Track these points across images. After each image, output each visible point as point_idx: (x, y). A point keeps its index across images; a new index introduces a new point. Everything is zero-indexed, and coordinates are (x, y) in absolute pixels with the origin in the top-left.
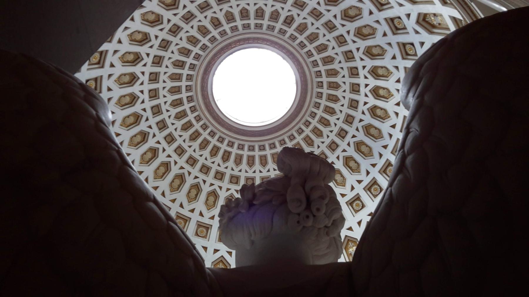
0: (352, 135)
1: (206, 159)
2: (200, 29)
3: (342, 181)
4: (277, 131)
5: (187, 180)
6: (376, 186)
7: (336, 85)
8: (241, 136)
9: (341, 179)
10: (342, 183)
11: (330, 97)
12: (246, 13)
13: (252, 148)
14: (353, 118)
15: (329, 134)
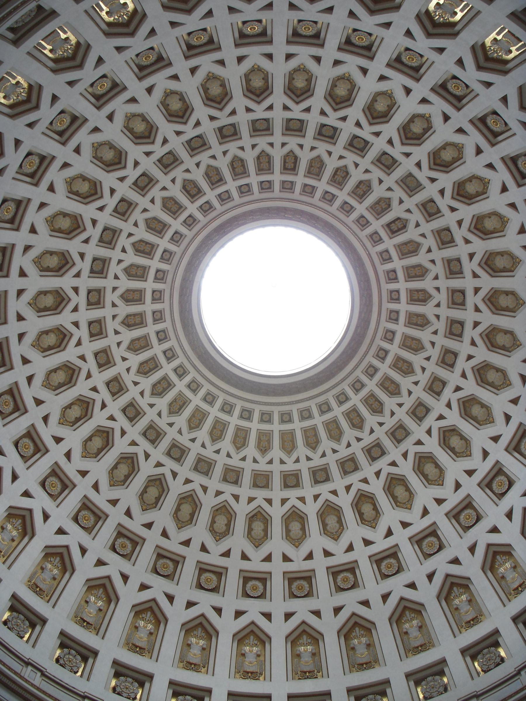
0: (390, 461)
1: (128, 370)
2: (261, 158)
3: (335, 530)
4: (267, 394)
5: (78, 383)
6: (392, 561)
7: (407, 368)
8: (207, 370)
9: (335, 526)
10: (335, 533)
11: (386, 382)
12: (342, 177)
13: (211, 399)
14: (408, 433)
15: (353, 442)
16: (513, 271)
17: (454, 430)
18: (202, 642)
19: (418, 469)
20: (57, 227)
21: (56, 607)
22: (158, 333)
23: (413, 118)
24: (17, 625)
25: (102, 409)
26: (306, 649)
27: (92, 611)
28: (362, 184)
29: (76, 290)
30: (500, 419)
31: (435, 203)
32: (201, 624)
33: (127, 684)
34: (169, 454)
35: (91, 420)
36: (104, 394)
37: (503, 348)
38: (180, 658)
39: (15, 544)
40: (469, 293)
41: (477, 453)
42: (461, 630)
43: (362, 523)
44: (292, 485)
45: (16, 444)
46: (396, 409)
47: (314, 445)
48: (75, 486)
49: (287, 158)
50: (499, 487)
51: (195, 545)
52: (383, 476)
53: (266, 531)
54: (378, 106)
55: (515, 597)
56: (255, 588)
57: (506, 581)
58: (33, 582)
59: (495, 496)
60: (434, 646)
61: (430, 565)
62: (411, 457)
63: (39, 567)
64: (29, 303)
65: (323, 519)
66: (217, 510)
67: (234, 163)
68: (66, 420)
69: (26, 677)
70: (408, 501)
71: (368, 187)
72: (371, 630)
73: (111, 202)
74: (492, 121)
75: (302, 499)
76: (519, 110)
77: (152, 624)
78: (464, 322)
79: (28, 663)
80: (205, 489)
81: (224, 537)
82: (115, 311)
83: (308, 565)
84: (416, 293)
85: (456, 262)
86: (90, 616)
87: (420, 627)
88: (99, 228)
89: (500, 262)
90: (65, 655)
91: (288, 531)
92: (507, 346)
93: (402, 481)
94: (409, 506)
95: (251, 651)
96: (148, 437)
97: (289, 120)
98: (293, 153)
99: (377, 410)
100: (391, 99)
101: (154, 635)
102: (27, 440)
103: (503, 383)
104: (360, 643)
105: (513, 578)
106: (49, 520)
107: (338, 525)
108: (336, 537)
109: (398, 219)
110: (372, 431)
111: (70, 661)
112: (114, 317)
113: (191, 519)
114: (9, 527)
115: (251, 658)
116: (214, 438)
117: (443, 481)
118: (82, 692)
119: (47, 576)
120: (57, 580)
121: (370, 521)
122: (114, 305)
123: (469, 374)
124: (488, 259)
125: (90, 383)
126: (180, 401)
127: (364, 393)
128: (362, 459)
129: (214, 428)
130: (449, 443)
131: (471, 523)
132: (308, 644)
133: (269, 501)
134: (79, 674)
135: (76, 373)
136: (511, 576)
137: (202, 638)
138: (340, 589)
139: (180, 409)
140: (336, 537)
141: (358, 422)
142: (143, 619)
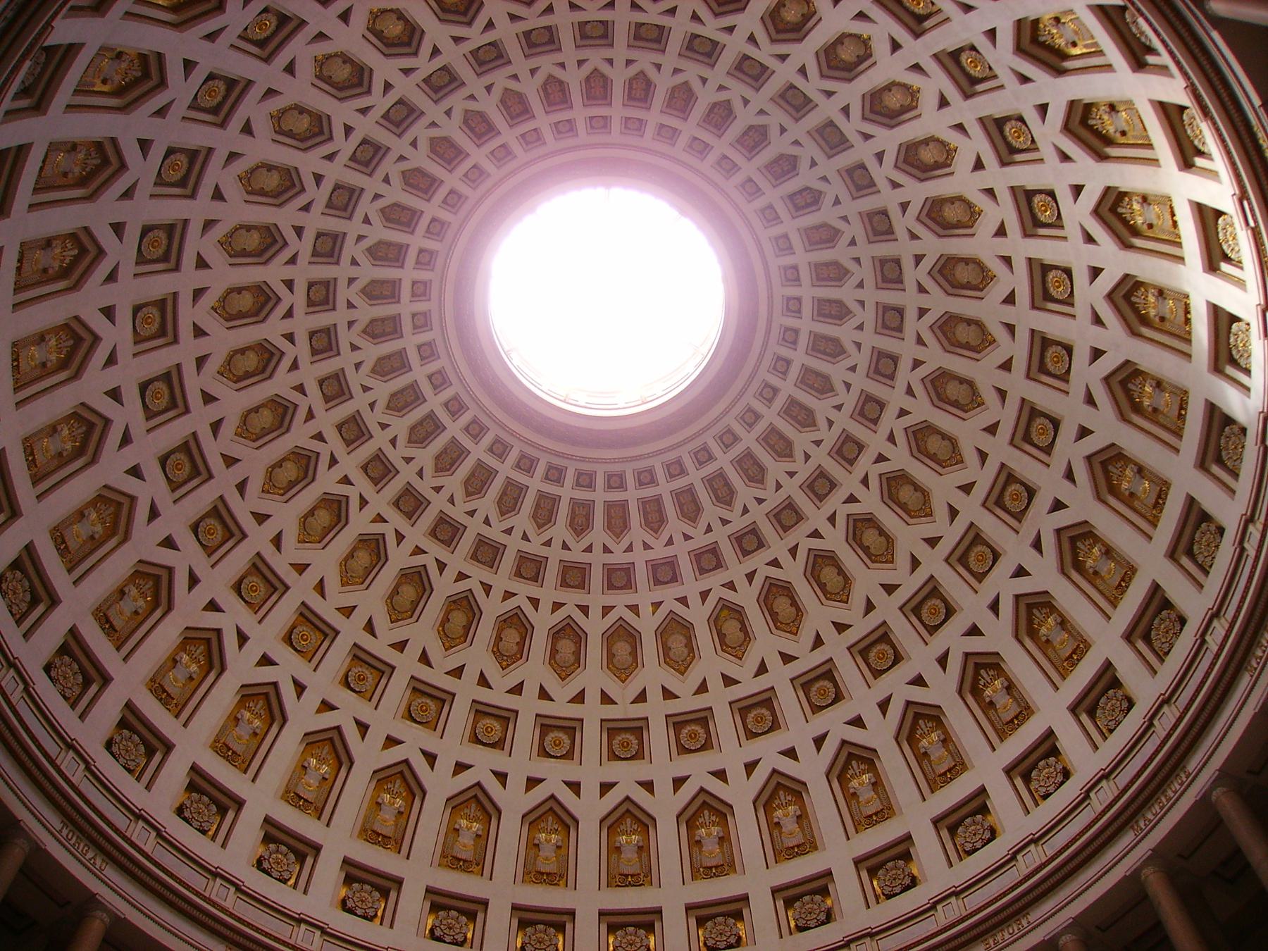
1: (372, 405)
2: (592, 80)
3: (682, 658)
14: (800, 517)
15: (716, 525)
16: (982, 290)
17: (869, 520)
18: (476, 826)
20: (257, 187)
21: (258, 781)
22: (419, 347)
23: (841, 39)
24: (199, 813)
25: (330, 467)
26: (629, 840)
27: (312, 781)
28: (754, 130)
29: (289, 284)
30: (941, 512)
31: (867, 170)
32: (475, 796)
33: (363, 894)
34: (433, 533)
35: (313, 484)
36: (335, 443)
37: (955, 404)
38: (443, 851)
39: (195, 683)
40: (911, 314)
41: (903, 561)
42: (858, 827)
43: (723, 650)
44: (620, 585)
45: (195, 528)
46: (784, 480)
48: (287, 588)
49: (634, 82)
50: (931, 616)
51: (470, 675)
52: (758, 580)
53: (577, 654)
54: (786, 14)
55: (941, 787)
56: (557, 744)
57: (930, 762)
58: (222, 741)
59: (923, 628)
60: (816, 848)
61: (820, 723)
62: (802, 554)
63: (232, 718)
64: (212, 307)
65: (664, 639)
66: (505, 621)
68: (274, 485)
69: (213, 897)
71: (762, 135)
72: (726, 815)
73: (346, 147)
74: (969, 60)
75: (634, 609)
76: (1014, 53)
77: (403, 799)
78: (898, 357)
79: (215, 874)
80: (487, 588)
81: (514, 662)
82: (353, 314)
83: (638, 711)
84: (828, 304)
85: (894, 264)
86: (309, 790)
87: (799, 817)
88: (327, 186)
89: (963, 274)
90: (271, 854)
91: (611, 656)
92: (962, 402)
93: (786, 589)
94: (794, 629)
95: (548, 841)
96: (402, 508)
97: (639, 25)
98: (645, 75)
100: (809, 6)
101: (405, 816)
102: (212, 522)
103: (952, 457)
104: (709, 835)
105: (940, 758)
106: (248, 644)
107: (686, 651)
108: (682, 668)
109: (807, 188)
110: (745, 510)
111: (278, 863)
112: (351, 324)
113: (466, 633)
114: (185, 658)
115: (547, 851)
116: (504, 509)
117: (848, 596)
118: (297, 913)
119: (243, 731)
120: (258, 737)
121: (735, 648)
122: (350, 305)
123: (900, 438)
124: (944, 266)
125: (313, 427)
127: (737, 450)
128: (727, 551)
129: (504, 493)
131: (884, 665)
132: (634, 832)
133: (584, 610)
134: (292, 881)
135: (290, 411)
136: (937, 755)
137: (476, 820)
138: (683, 750)
139: (452, 465)
140: (682, 668)
141: (725, 495)
142: (388, 791)
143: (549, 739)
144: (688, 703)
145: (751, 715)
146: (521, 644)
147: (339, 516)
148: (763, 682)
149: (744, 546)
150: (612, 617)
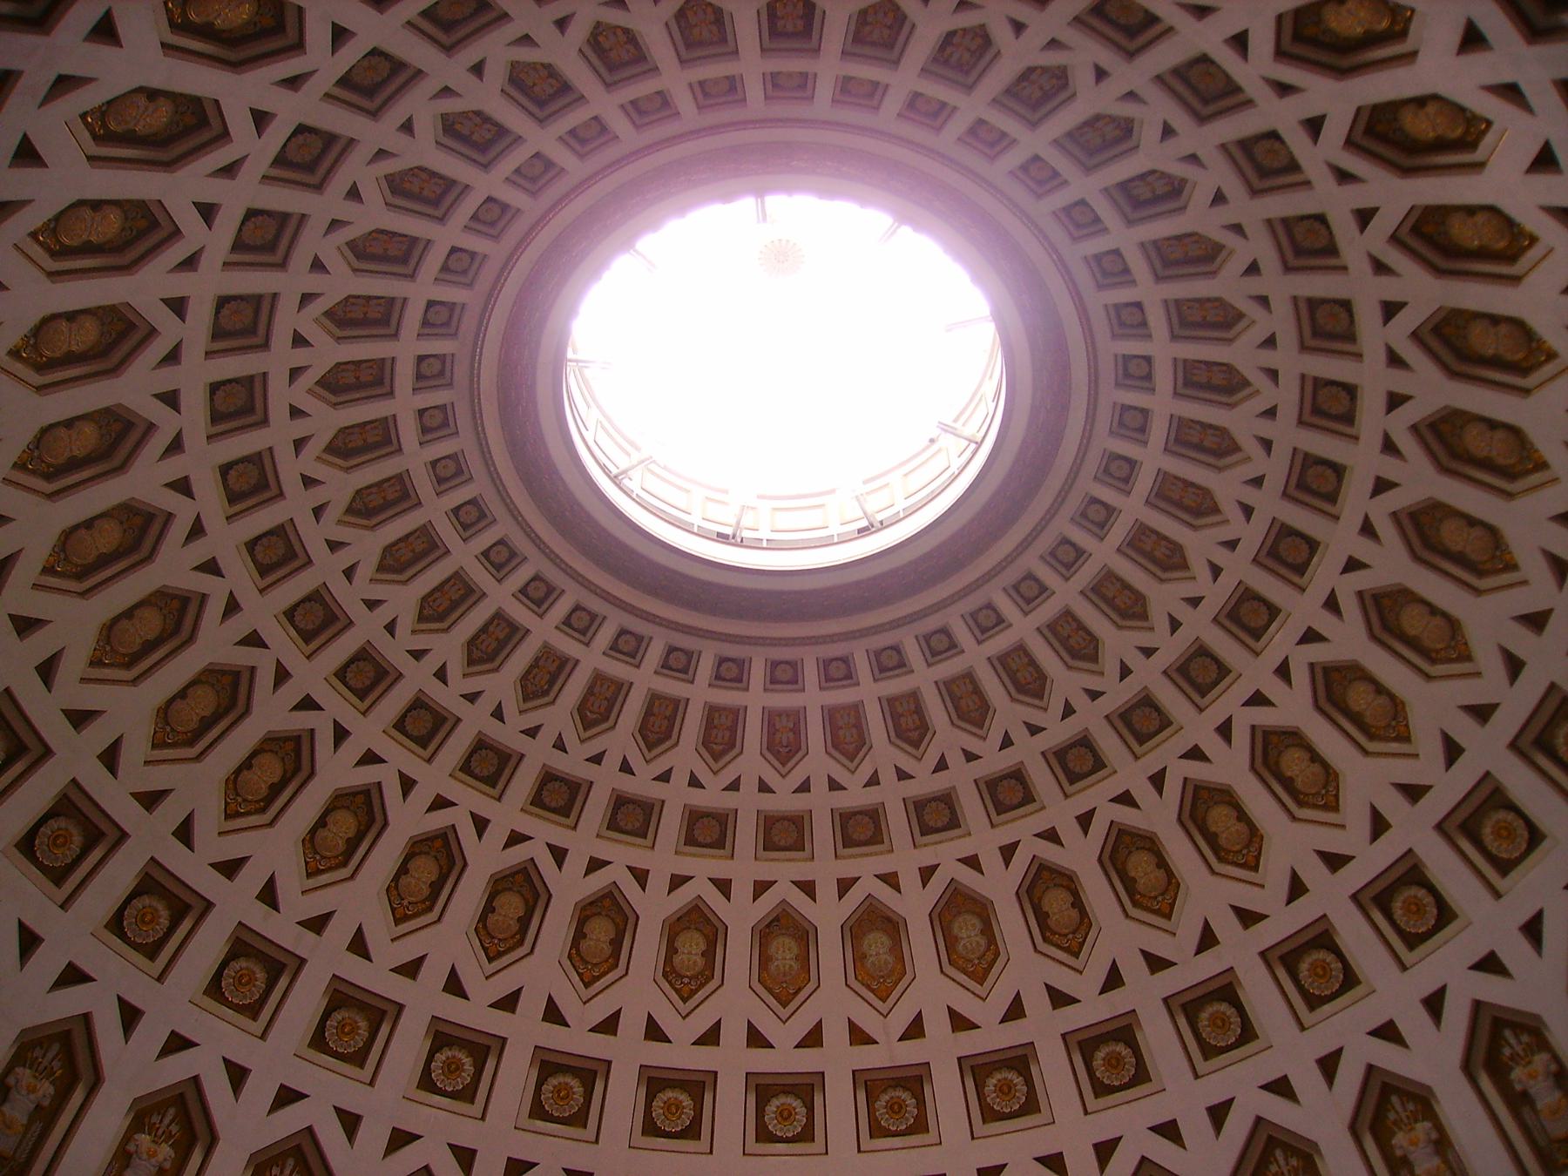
2: (689, 14)
3: (977, 955)
10: (976, 962)
15: (1019, 735)
19: (1192, 817)
43: (1045, 939)
47: (914, 735)
56: (785, 1115)
67: (601, 39)
70: (1162, 894)
75: (891, 880)
99: (1083, 652)
121: (1066, 935)
126: (550, 661)
130: (1277, 763)
133: (808, 888)
139: (552, 683)
143: (772, 1108)
144: (994, 1037)
145: (1100, 1055)
146: (709, 954)
147: (370, 812)
148: (1118, 1002)
149: (1071, 765)
150: (856, 895)
